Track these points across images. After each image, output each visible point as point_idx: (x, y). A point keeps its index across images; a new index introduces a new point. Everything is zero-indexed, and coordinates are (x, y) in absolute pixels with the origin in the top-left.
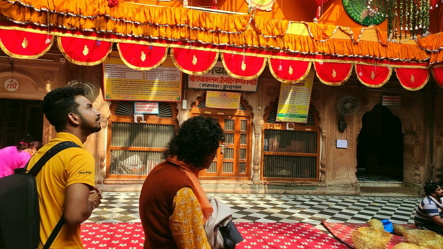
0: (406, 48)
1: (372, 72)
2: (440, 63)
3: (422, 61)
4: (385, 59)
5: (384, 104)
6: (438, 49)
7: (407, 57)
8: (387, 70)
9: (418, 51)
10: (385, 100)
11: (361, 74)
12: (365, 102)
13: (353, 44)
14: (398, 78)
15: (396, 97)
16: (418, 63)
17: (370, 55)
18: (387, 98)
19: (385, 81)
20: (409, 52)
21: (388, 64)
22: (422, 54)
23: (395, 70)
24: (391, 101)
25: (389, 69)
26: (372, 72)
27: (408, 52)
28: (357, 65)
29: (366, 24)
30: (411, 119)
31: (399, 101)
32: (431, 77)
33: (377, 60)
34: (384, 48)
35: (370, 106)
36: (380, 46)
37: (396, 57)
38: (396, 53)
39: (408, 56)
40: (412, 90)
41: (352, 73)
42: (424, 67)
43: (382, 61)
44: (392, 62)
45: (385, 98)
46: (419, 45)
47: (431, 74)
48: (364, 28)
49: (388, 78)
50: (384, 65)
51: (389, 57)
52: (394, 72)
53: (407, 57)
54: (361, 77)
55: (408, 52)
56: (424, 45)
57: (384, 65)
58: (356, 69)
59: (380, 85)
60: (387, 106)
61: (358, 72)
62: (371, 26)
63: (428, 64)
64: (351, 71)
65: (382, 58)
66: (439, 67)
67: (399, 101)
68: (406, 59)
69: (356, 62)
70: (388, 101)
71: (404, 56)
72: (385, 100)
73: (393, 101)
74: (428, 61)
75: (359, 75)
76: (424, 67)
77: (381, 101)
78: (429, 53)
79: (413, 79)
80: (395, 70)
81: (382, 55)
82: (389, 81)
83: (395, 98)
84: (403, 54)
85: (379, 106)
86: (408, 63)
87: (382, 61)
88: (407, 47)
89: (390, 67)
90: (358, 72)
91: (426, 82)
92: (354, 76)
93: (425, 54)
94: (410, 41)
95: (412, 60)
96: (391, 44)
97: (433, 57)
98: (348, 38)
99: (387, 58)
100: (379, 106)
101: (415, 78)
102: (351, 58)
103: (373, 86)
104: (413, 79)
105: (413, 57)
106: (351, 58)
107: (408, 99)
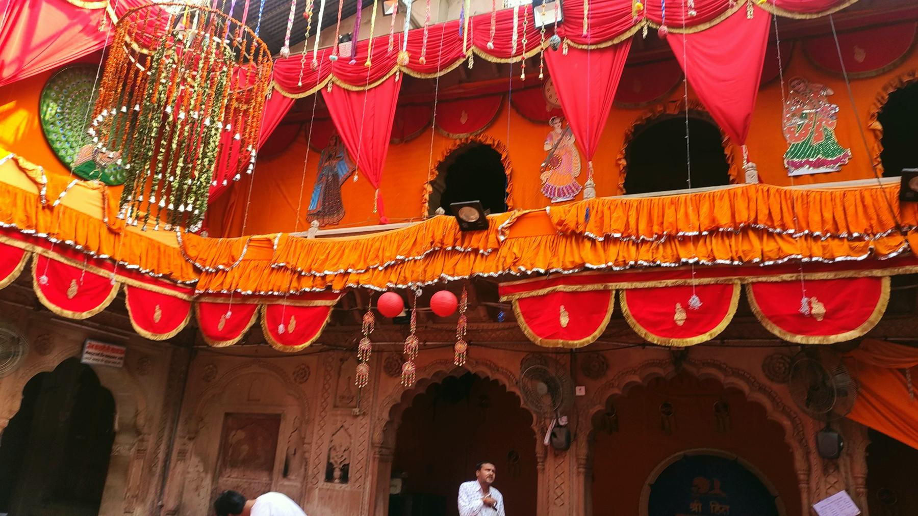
0: (156, 251)
1: (74, 282)
2: (212, 295)
3: (183, 283)
4: (109, 262)
5: (86, 359)
6: (214, 268)
7: (156, 269)
8: (106, 285)
9: (180, 261)
10: (90, 350)
11: (44, 279)
12: (41, 348)
13: (40, 206)
14: (128, 307)
15: (116, 347)
16: (174, 286)
17: (76, 243)
18: (97, 348)
19: (97, 308)
20: (162, 260)
21: (112, 271)
22: (185, 270)
23: (125, 288)
24: (102, 355)
25: (113, 283)
26: (74, 282)
27: (159, 259)
28: (41, 257)
29: (85, 176)
30: (138, 402)
31: (121, 358)
32: (193, 318)
33: (89, 258)
34: (112, 237)
35: (52, 361)
36: (104, 231)
37: (133, 263)
38: (134, 254)
39: (159, 266)
40: (152, 338)
41: (22, 272)
42: (184, 296)
43: (100, 263)
44: (122, 270)
45: (91, 347)
46: (184, 251)
47: (194, 313)
48: (76, 181)
49: (107, 303)
50: (103, 272)
51: (118, 258)
52: (121, 294)
53: (156, 269)
54: (43, 288)
55: (159, 259)
56: (192, 253)
57: (103, 272)
58: (34, 266)
59: (85, 315)
60: (93, 365)
61: (40, 274)
62: (95, 183)
63: (191, 293)
64: (21, 266)
65: (102, 256)
66: (210, 301)
67: (121, 358)
68: (153, 271)
69: (39, 250)
70: (98, 355)
71: (149, 265)
72: (90, 350)
73: (107, 356)
74: (194, 285)
75: (38, 280)
76: (184, 296)
77: (82, 356)
78: (198, 271)
79: (158, 315)
80: (125, 288)
81: (104, 248)
82: (106, 309)
83: (114, 350)
84: (150, 259)
85: (72, 364)
86: (155, 281)
87: (100, 263)
88: (159, 248)
89: (116, 279)
90: (40, 274)
91: (182, 326)
92: (25, 280)
93: (191, 270)
94: (168, 237)
95: (164, 276)
96: (129, 234)
97: (203, 280)
98: (32, 189)
99: (112, 259)
100: (72, 364)
101: (163, 314)
102: (27, 238)
103: (68, 314)
104: (158, 315)
105: (167, 272)
106: (27, 238)
107: (139, 356)
